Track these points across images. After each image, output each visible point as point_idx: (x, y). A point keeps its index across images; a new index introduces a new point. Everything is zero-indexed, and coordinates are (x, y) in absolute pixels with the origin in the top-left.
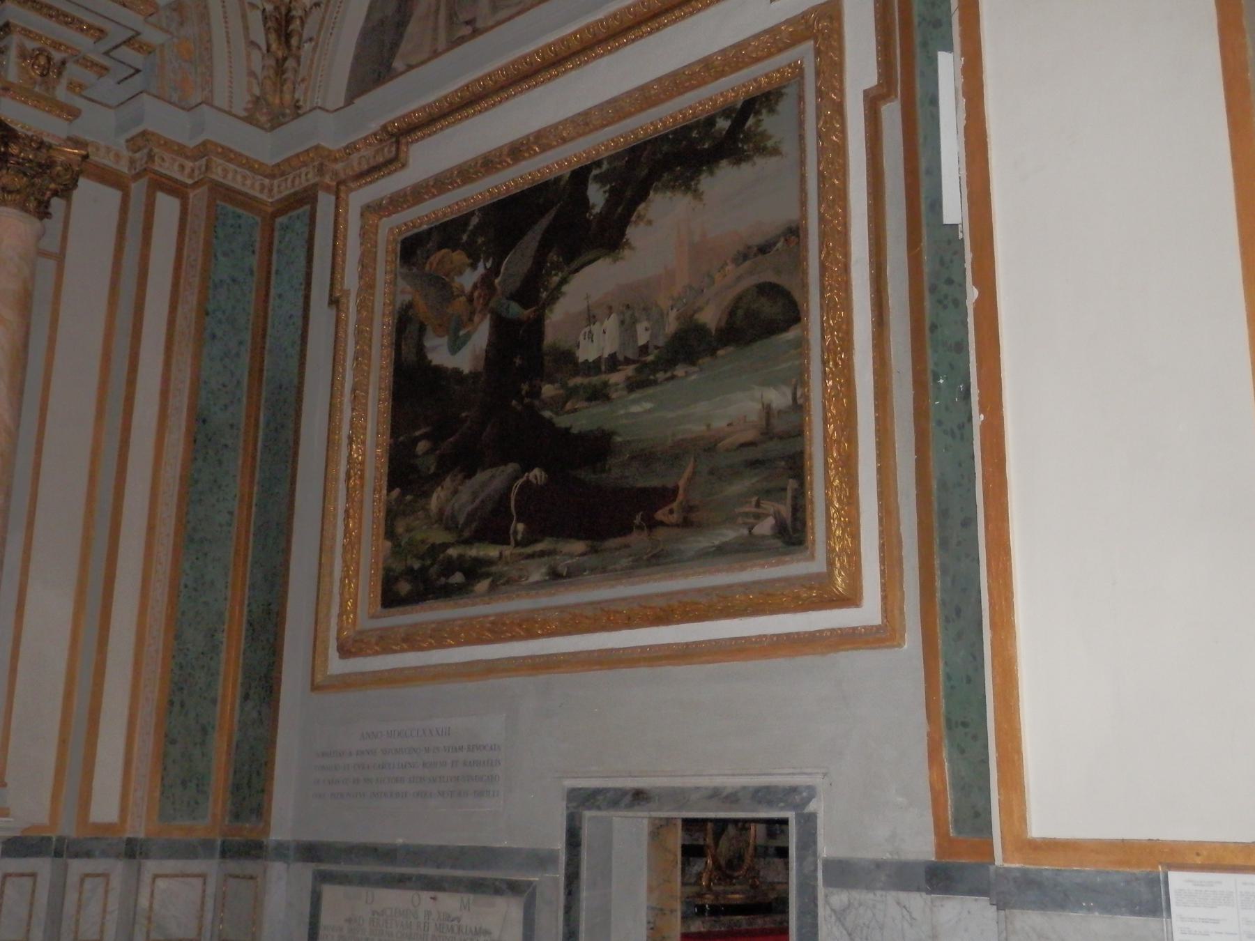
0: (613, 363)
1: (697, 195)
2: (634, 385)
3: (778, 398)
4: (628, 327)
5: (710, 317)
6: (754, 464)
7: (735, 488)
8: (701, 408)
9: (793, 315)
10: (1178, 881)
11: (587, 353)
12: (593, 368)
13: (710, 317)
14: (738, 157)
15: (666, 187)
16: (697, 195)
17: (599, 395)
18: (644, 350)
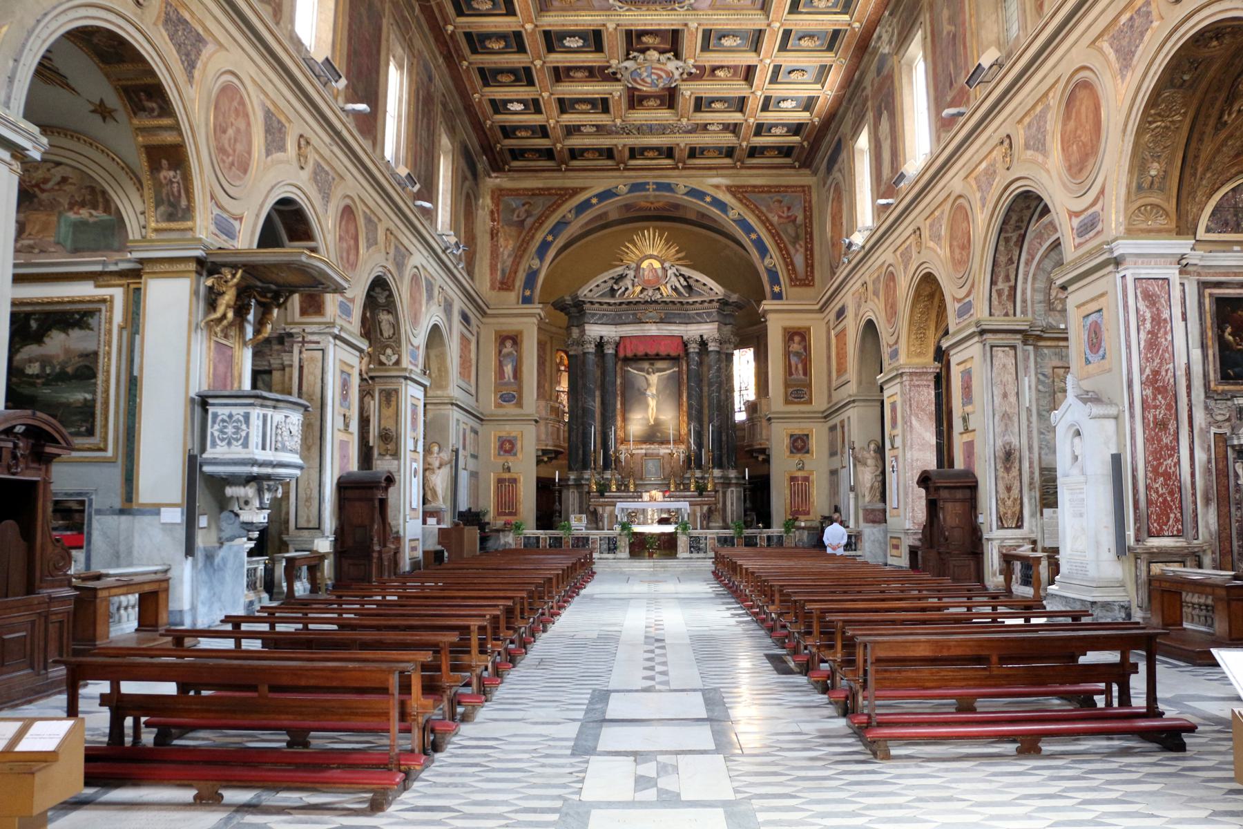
0: (38, 376)
1: (68, 334)
2: (44, 384)
3: (89, 396)
4: (43, 367)
5: (69, 370)
6: (81, 413)
7: (74, 418)
8: (66, 395)
9: (94, 376)
10: (163, 509)
11: (29, 371)
12: (31, 376)
13: (69, 370)
14: (81, 328)
15: (58, 329)
16: (68, 334)
17: (33, 385)
18: (49, 375)
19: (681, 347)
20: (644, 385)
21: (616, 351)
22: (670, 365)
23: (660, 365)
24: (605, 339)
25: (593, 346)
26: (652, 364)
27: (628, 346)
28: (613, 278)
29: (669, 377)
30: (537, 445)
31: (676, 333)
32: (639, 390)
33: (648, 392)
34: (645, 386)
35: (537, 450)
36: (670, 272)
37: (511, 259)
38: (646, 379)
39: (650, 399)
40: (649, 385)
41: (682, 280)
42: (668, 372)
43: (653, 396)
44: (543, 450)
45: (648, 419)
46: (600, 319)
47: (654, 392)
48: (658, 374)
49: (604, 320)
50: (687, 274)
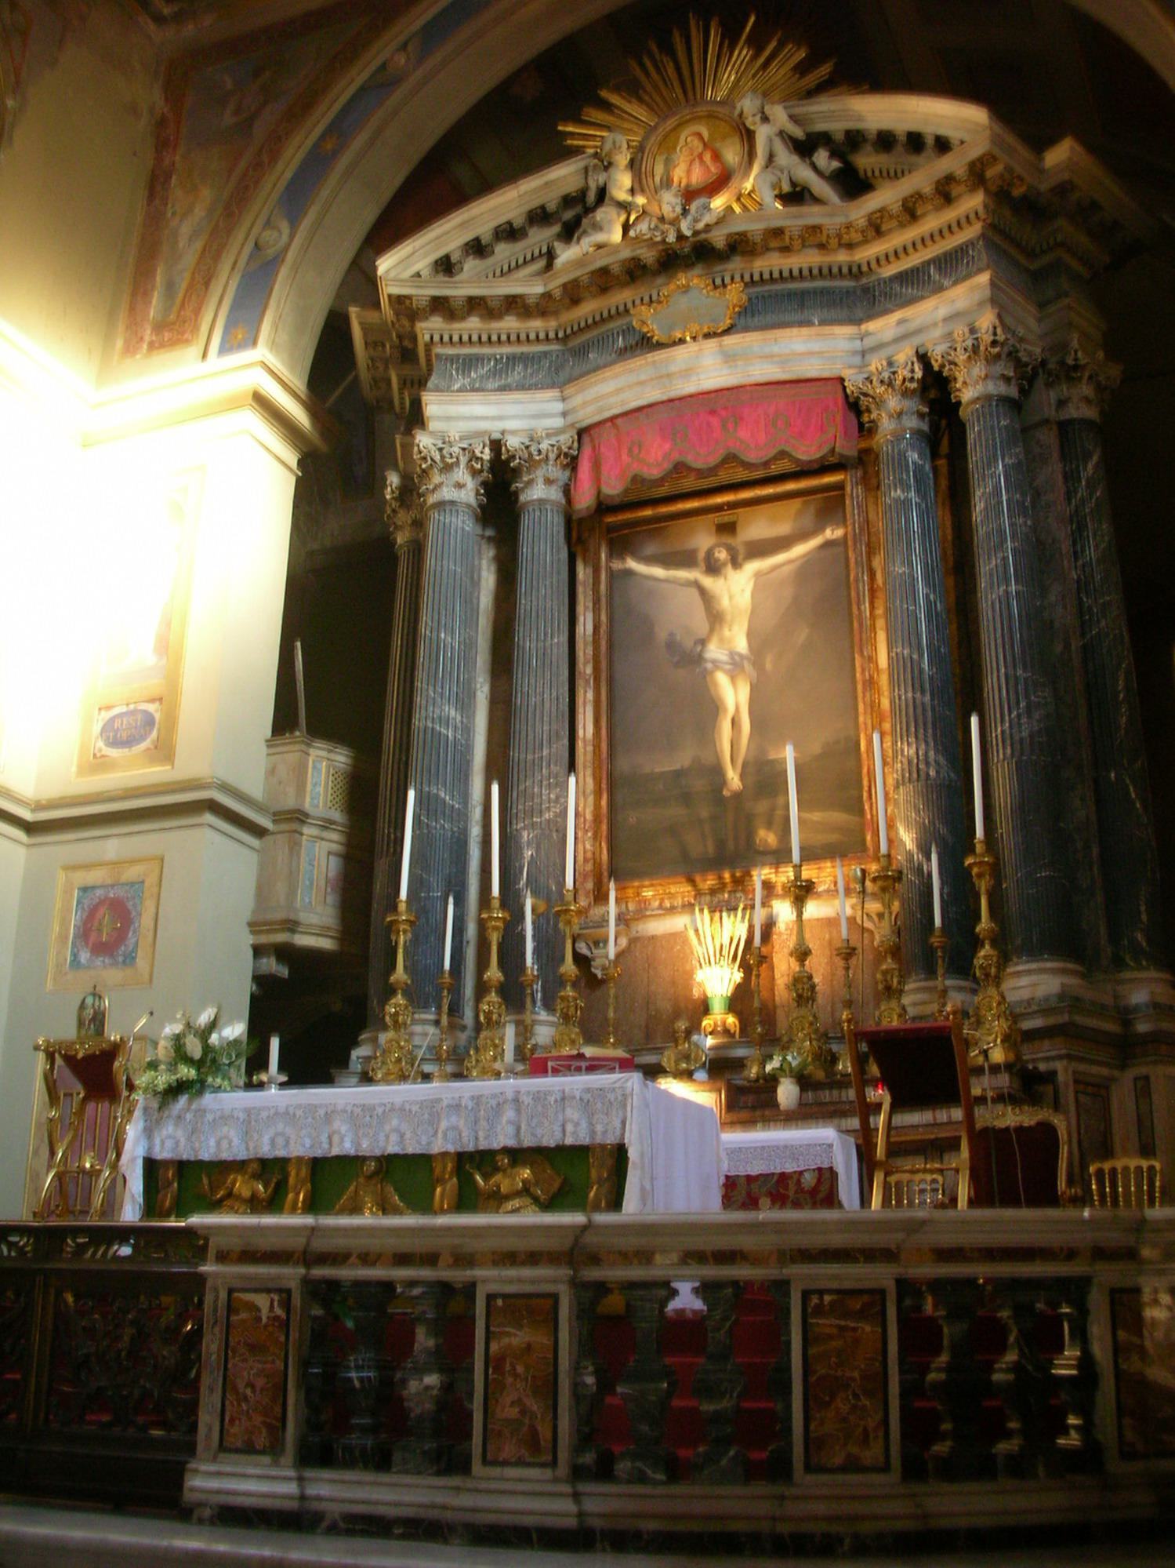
19: (839, 412)
20: (699, 622)
21: (567, 491)
22: (808, 520)
23: (758, 527)
24: (513, 442)
25: (462, 474)
26: (728, 529)
27: (608, 455)
28: (539, 216)
29: (805, 570)
30: (254, 926)
31: (812, 368)
32: (671, 645)
33: (714, 651)
34: (699, 622)
35: (258, 951)
36: (763, 133)
37: (198, 245)
38: (703, 592)
39: (722, 679)
40: (716, 618)
41: (822, 157)
42: (800, 550)
43: (735, 667)
44: (284, 952)
45: (718, 771)
46: (495, 373)
47: (741, 645)
48: (752, 567)
49: (516, 374)
50: (836, 128)
